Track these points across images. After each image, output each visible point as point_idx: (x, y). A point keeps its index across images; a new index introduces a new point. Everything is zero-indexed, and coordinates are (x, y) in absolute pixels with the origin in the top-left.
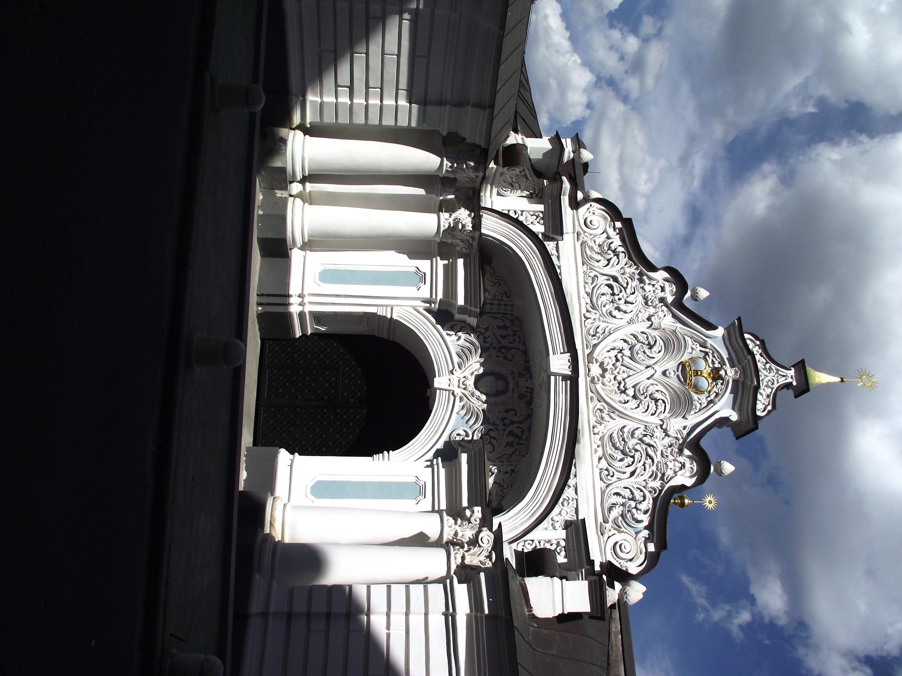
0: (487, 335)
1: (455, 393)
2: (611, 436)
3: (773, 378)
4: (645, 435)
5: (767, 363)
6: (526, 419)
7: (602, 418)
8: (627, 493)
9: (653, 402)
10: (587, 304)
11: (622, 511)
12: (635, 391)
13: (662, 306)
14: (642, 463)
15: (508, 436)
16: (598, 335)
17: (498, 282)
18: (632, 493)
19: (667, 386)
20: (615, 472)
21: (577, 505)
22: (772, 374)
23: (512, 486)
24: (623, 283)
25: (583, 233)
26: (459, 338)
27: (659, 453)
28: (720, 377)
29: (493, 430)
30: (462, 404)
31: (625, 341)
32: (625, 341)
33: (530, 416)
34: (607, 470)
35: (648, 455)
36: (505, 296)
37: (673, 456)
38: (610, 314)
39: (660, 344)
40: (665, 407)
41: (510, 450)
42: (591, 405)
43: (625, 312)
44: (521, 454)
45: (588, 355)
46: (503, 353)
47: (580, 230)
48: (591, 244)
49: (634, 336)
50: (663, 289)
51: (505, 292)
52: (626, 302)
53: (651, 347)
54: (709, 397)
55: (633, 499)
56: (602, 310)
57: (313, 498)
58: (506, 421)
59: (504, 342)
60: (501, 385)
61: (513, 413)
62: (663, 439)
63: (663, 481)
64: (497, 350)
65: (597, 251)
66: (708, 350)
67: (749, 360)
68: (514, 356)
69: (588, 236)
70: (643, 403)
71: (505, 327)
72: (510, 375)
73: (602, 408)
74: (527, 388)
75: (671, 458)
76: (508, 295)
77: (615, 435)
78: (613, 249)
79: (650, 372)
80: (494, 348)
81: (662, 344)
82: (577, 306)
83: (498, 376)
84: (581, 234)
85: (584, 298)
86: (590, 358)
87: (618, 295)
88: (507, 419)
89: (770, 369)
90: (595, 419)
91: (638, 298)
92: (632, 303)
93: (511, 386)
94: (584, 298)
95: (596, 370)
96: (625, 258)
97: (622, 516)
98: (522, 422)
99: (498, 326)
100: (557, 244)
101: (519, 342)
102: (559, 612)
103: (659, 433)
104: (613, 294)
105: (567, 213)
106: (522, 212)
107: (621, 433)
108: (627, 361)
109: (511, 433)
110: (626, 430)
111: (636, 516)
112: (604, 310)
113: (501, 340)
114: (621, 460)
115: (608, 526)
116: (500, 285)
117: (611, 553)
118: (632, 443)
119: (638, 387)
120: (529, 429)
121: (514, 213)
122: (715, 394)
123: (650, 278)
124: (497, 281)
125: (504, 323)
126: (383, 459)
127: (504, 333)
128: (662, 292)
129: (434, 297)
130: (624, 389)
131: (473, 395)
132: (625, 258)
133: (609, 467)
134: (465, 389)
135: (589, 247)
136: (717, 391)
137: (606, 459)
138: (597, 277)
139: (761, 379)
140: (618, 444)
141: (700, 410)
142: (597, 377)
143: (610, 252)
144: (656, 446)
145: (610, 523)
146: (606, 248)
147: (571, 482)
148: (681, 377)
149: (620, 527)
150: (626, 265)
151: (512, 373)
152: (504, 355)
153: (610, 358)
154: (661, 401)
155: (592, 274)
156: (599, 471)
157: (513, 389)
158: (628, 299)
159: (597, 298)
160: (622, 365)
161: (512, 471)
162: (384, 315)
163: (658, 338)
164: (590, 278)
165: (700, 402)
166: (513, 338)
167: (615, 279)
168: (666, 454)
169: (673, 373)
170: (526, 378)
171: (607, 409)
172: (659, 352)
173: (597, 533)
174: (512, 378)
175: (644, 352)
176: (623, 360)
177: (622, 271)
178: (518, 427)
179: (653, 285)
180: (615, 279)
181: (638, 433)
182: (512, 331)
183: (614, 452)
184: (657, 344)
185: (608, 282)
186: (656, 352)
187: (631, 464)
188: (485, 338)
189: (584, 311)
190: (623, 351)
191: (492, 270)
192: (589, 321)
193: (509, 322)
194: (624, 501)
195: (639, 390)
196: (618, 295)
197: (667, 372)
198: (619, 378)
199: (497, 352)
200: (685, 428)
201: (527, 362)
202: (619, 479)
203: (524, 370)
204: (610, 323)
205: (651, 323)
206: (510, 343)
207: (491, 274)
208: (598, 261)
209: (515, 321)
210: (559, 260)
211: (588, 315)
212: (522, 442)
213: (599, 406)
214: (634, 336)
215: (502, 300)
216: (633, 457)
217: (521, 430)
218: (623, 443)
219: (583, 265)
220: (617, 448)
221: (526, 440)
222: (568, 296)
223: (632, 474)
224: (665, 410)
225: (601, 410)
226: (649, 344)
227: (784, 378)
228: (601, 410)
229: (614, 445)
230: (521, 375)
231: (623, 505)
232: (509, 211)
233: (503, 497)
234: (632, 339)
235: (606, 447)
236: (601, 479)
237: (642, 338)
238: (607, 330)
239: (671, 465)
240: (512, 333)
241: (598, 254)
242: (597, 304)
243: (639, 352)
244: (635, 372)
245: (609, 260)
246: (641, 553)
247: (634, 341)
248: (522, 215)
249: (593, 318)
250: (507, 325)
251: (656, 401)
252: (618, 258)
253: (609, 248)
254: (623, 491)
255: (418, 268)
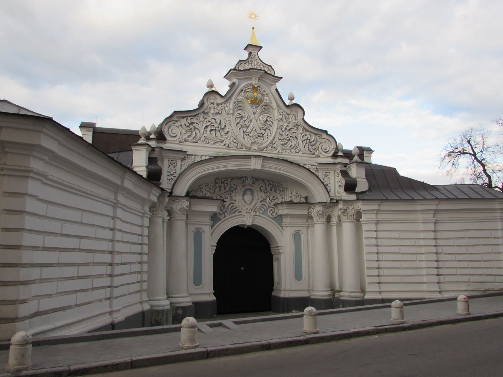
0: (224, 197)
1: (254, 215)
2: (282, 145)
3: (256, 62)
4: (282, 129)
5: (248, 62)
6: (264, 182)
7: (275, 147)
8: (305, 142)
9: (268, 122)
10: (220, 145)
11: (311, 146)
12: (262, 129)
13: (221, 106)
14: (293, 133)
15: (272, 191)
16: (237, 142)
17: (200, 188)
18: (304, 140)
19: (261, 114)
20: (296, 146)
21: (310, 165)
22: (254, 62)
23: (297, 192)
24: (209, 124)
25: (180, 140)
26: (226, 211)
27: (289, 125)
28: (257, 88)
29: (270, 198)
30: (258, 212)
31: (240, 129)
32: (240, 129)
33: (263, 180)
34: (295, 149)
35: (289, 130)
36: (208, 186)
37: (290, 119)
38: (226, 134)
39: (241, 112)
40: (269, 117)
41: (278, 191)
42: (269, 152)
43: (225, 126)
44: (279, 186)
45: (246, 149)
46: (233, 190)
47: (177, 141)
48: (186, 136)
49: (238, 123)
50: (213, 104)
51: (206, 186)
52: (220, 124)
53: (242, 117)
54: (264, 95)
55: (306, 140)
56: (225, 138)
57: (303, 279)
58: (265, 191)
59: (228, 188)
60: (249, 192)
61: (262, 188)
62: (283, 121)
63: (299, 125)
64: (232, 193)
65: (190, 134)
66: (244, 90)
67: (252, 71)
68: (234, 185)
69: (181, 137)
70: (268, 127)
71: (220, 187)
72: (244, 188)
73: (271, 147)
74: (250, 180)
75: (290, 120)
76: (208, 184)
77: (282, 143)
78: (189, 124)
79: (254, 120)
80: (231, 194)
81: (241, 111)
82: (220, 150)
83: (244, 194)
84: (180, 141)
85: (217, 146)
86: (248, 148)
87: (216, 128)
88: (264, 191)
89: (251, 61)
90: (275, 151)
91: (217, 117)
92: (221, 121)
93: (250, 187)
94: (217, 146)
95: (255, 147)
96: (194, 119)
97: (312, 146)
98: (266, 184)
99: (219, 191)
100: (187, 155)
101: (227, 181)
102: (365, 180)
103: (281, 123)
104: (215, 130)
105: (166, 146)
106: (168, 172)
107: (281, 140)
108: (249, 130)
109: (271, 189)
110: (280, 138)
111: (312, 140)
112: (224, 136)
113: (226, 190)
114: (291, 142)
115: (316, 153)
116: (202, 188)
117: (328, 154)
118: (285, 137)
119: (261, 128)
120: (268, 181)
121: (169, 177)
122: (264, 92)
123: (206, 109)
124: (200, 189)
125: (218, 188)
126: (282, 249)
127: (222, 189)
128: (214, 104)
129: (209, 224)
130: (262, 135)
131: (254, 206)
132: (194, 119)
133: (294, 148)
134: (251, 210)
135: (188, 138)
136: (263, 91)
137: (291, 149)
138: (204, 137)
139: (256, 68)
140: (285, 142)
141: (270, 101)
142: (258, 146)
143: (191, 127)
144: (286, 126)
145: (315, 152)
146: (189, 129)
147: (303, 165)
148: (256, 106)
149: (316, 148)
150: (197, 119)
151: (243, 186)
152: (234, 189)
153: (248, 139)
154: (267, 119)
155: (204, 139)
156: (296, 153)
157: (251, 186)
158: (219, 123)
159: (218, 139)
160: (251, 133)
161: (291, 191)
162: (215, 250)
163: (238, 112)
164: (206, 141)
165: (267, 100)
166: (225, 184)
167: (206, 127)
168: (289, 122)
169: (254, 109)
170: (246, 180)
171: (271, 145)
172: (244, 113)
173: (319, 158)
174: (246, 186)
175: (245, 121)
176: (248, 132)
177: (202, 122)
178: (268, 186)
179: (210, 108)
180: (206, 127)
181: (281, 133)
182: (221, 184)
183: (289, 145)
184: (241, 113)
185: (208, 132)
186: (245, 116)
187: (293, 138)
188: (225, 198)
189: (224, 147)
190: (245, 131)
191: (193, 192)
192: (230, 146)
193: (216, 185)
194: (307, 145)
195: (262, 127)
196: (216, 128)
197: (254, 112)
198: (257, 136)
199: (233, 193)
200: (278, 110)
201: (237, 179)
202: (298, 145)
203: (241, 180)
204: (231, 135)
205: (231, 115)
206: (228, 186)
207: (195, 192)
208: (196, 135)
209: (216, 182)
210: (198, 155)
211: (227, 145)
212: (274, 185)
213: (269, 148)
214: (238, 123)
215: (210, 188)
216: (290, 136)
217: (269, 185)
218: (285, 140)
219: (197, 142)
220: (287, 143)
221: (273, 183)
222: (218, 154)
223: (296, 138)
224: (271, 117)
225: (272, 147)
226: (240, 117)
227: (255, 56)
228: (272, 147)
229: (285, 144)
230: (243, 182)
231: (308, 145)
232: (168, 179)
233: (301, 196)
234: (239, 126)
235: (287, 148)
236: (298, 152)
237: (238, 121)
238: (234, 137)
239: (294, 121)
240: (223, 184)
241: (191, 133)
242: (221, 139)
243: (245, 123)
244: (254, 128)
245: (195, 128)
246: (326, 141)
247: (240, 125)
248: (170, 172)
249: (228, 143)
250: (219, 186)
251: (267, 121)
252: (194, 123)
253: (188, 126)
254: (303, 145)
255: (192, 232)
